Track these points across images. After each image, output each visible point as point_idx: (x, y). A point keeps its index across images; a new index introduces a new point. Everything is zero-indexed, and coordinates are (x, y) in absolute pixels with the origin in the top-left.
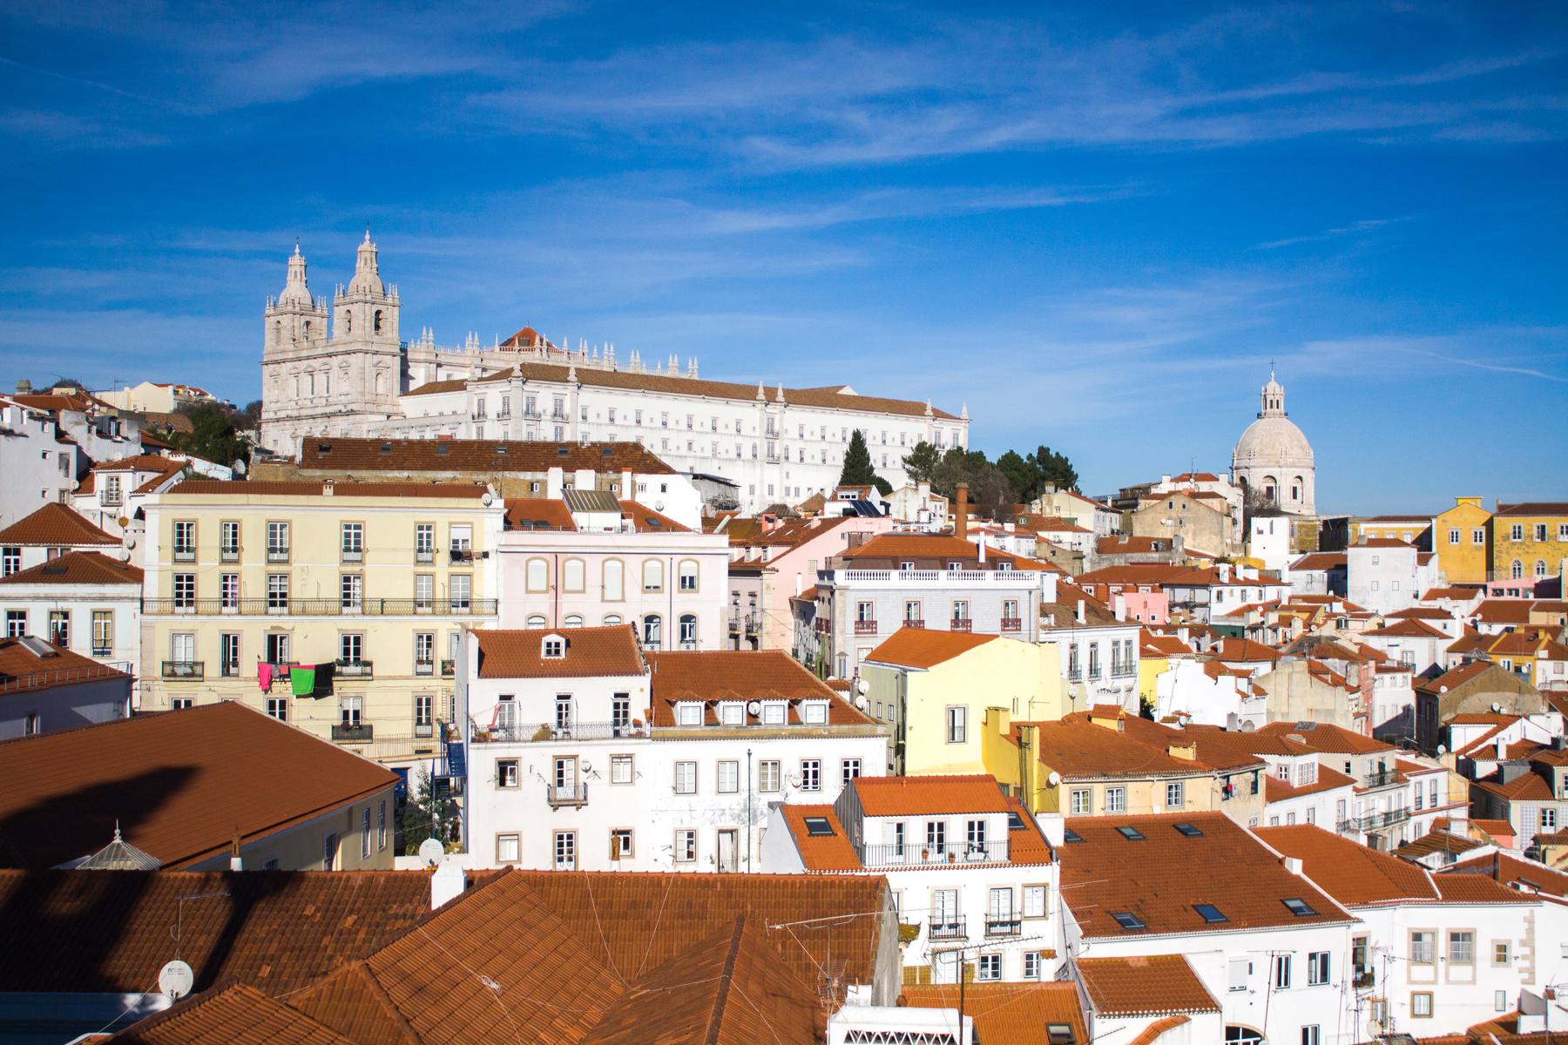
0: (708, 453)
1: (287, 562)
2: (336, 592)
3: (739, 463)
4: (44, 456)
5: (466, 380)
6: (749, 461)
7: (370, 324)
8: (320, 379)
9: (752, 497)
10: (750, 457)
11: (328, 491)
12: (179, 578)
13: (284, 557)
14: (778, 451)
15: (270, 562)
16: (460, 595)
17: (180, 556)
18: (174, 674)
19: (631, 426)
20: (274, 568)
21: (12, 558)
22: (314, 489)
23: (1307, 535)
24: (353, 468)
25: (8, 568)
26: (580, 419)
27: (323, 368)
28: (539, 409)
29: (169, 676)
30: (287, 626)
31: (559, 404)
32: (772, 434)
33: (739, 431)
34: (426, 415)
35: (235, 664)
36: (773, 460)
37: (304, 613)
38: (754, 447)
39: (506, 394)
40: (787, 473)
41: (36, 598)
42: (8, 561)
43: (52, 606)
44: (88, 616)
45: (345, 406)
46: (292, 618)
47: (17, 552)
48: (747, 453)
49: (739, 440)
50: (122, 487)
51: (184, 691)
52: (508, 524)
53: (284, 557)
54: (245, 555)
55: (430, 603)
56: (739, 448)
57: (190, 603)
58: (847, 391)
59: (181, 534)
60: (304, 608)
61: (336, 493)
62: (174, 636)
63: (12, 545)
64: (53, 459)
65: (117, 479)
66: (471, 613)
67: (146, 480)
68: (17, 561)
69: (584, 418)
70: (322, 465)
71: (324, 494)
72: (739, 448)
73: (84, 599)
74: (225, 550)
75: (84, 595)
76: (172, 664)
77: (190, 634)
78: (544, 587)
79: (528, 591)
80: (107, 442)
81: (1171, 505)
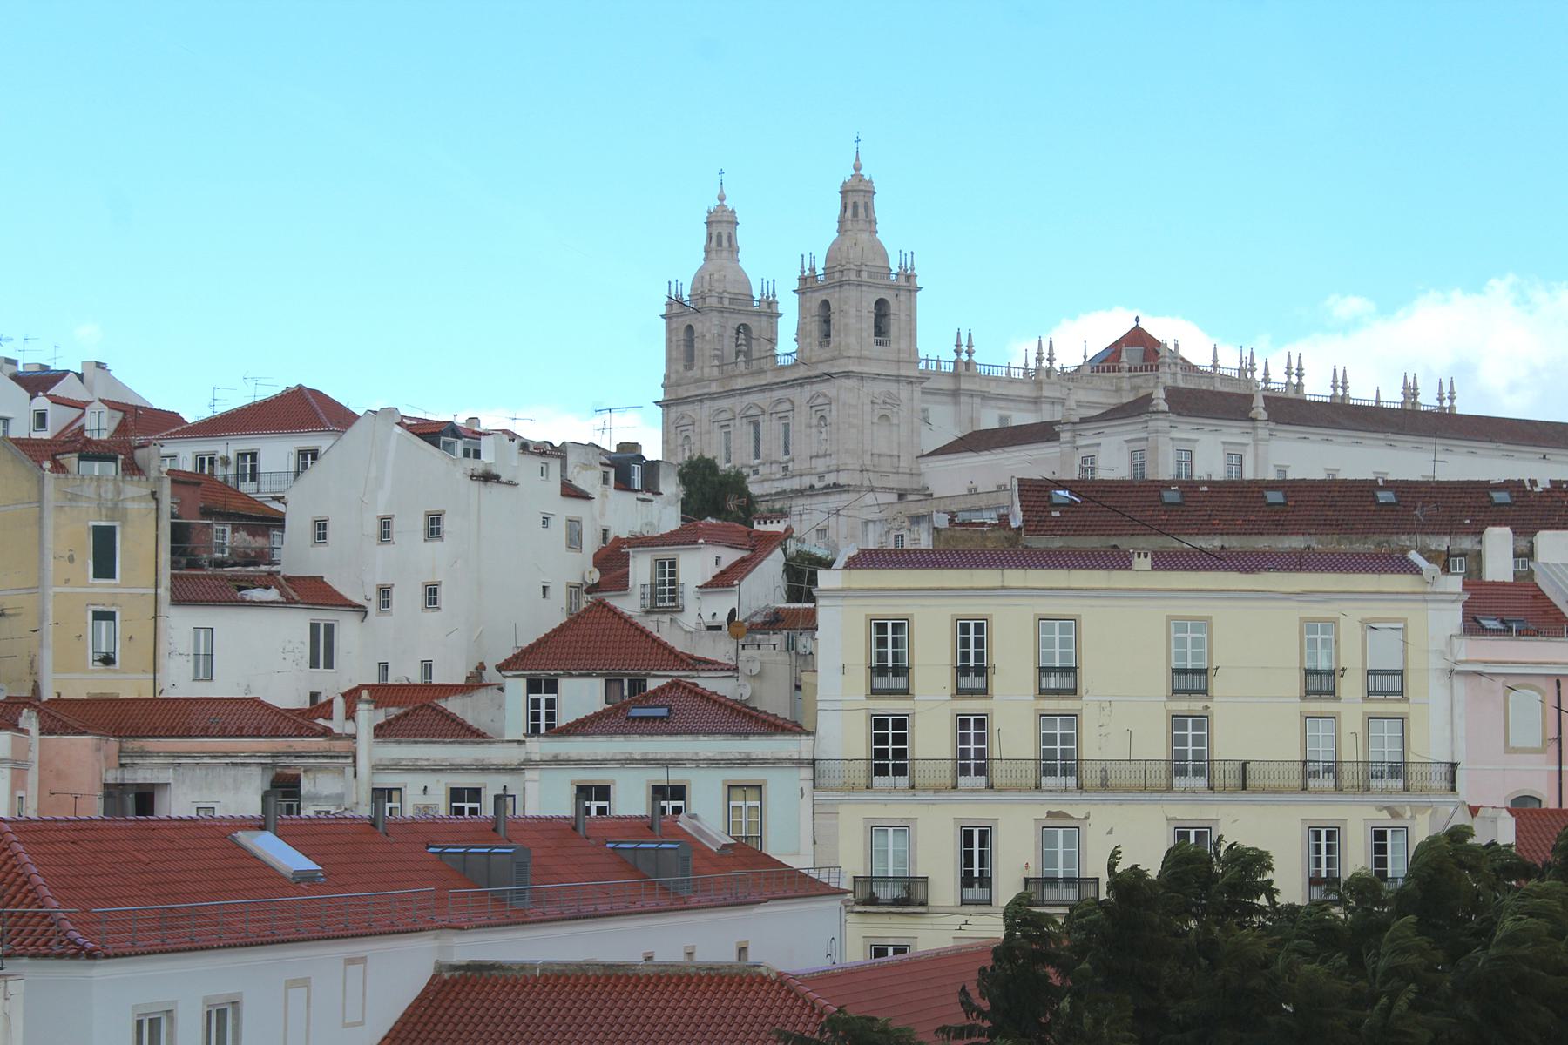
1: (1073, 692)
2: (1155, 745)
4: (546, 521)
5: (1058, 422)
8: (771, 430)
11: (1143, 563)
12: (880, 723)
13: (1067, 682)
15: (1043, 692)
16: (1386, 751)
17: (881, 682)
18: (872, 900)
20: (1052, 705)
21: (543, 697)
22: (1121, 561)
25: (536, 717)
27: (779, 408)
29: (865, 903)
30: (1077, 812)
34: (973, 491)
35: (985, 881)
37: (1105, 786)
39: (1137, 446)
41: (628, 762)
42: (536, 703)
43: (659, 776)
44: (720, 793)
45: (821, 478)
46: (1085, 797)
47: (552, 686)
50: (682, 577)
51: (891, 929)
52: (1472, 625)
53: (1067, 682)
54: (997, 683)
55: (1333, 768)
57: (900, 771)
59: (882, 642)
60: (1105, 778)
61: (1156, 566)
62: (877, 828)
63: (542, 675)
64: (559, 529)
65: (673, 564)
66: (1406, 789)
67: (724, 565)
68: (550, 704)
70: (1059, 528)
71: (1136, 567)
73: (713, 763)
74: (963, 671)
75: (710, 755)
76: (870, 880)
77: (904, 828)
78: (1536, 742)
79: (1509, 750)
80: (629, 497)
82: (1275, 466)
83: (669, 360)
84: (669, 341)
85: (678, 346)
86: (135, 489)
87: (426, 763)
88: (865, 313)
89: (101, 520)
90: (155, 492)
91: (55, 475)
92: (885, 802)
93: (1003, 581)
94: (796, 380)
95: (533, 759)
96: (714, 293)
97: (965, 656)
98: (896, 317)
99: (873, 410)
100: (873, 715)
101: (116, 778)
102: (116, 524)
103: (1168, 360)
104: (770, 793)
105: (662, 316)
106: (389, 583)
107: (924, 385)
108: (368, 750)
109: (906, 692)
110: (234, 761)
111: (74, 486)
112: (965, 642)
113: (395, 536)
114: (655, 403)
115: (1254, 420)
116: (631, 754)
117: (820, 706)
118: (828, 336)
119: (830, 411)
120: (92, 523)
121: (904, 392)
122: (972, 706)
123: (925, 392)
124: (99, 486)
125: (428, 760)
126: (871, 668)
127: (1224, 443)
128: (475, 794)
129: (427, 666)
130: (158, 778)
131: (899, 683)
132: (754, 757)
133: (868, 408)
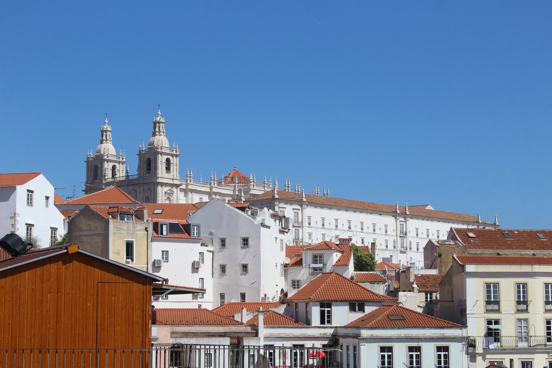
7: (164, 166)
10: (393, 248)
17: (490, 307)
19: (333, 229)
21: (326, 309)
24: (498, 248)
26: (307, 225)
33: (386, 232)
38: (394, 242)
47: (329, 306)
49: (387, 238)
54: (530, 308)
56: (387, 241)
58: (429, 208)
59: (489, 292)
68: (329, 312)
69: (309, 224)
72: (387, 241)
74: (519, 303)
82: (308, 216)
83: (88, 177)
84: (88, 170)
85: (91, 172)
86: (140, 226)
87: (283, 335)
88: (163, 163)
89: (128, 238)
90: (147, 228)
91: (113, 221)
92: (494, 354)
93: (532, 269)
94: (138, 184)
95: (364, 336)
96: (106, 155)
97: (519, 297)
98: (172, 164)
99: (165, 195)
100: (487, 319)
101: (173, 342)
102: (134, 240)
103: (252, 180)
104: (451, 350)
105: (85, 162)
106: (224, 263)
107: (181, 187)
108: (263, 331)
109: (498, 311)
110: (209, 334)
111: (119, 225)
112: (519, 292)
113: (227, 245)
114: (82, 190)
116: (400, 334)
117: (468, 316)
118: (150, 170)
119: (151, 195)
120: (125, 239)
121: (175, 189)
122: (523, 316)
123: (182, 190)
124: (128, 225)
125: (284, 334)
126: (486, 301)
127: (293, 209)
128: (302, 346)
129: (243, 296)
130: (189, 342)
131: (496, 307)
132: (446, 335)
133: (164, 194)
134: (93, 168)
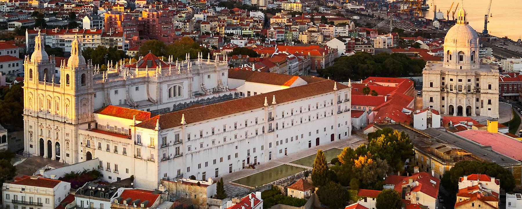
0: (244, 137)
3: (257, 137)
6: (261, 135)
9: (262, 152)
10: (262, 133)
14: (274, 126)
23: (517, 172)
26: (187, 140)
28: (168, 141)
31: (177, 136)
32: (271, 119)
36: (271, 130)
38: (263, 128)
40: (277, 135)
48: (260, 132)
81: (473, 205)
88: (79, 79)
115: (182, 124)
134: (29, 71)
